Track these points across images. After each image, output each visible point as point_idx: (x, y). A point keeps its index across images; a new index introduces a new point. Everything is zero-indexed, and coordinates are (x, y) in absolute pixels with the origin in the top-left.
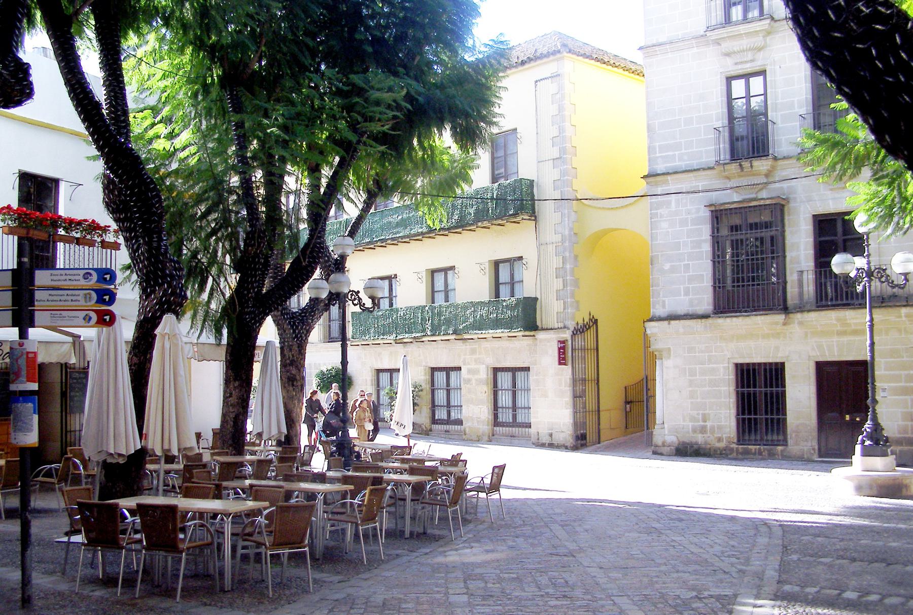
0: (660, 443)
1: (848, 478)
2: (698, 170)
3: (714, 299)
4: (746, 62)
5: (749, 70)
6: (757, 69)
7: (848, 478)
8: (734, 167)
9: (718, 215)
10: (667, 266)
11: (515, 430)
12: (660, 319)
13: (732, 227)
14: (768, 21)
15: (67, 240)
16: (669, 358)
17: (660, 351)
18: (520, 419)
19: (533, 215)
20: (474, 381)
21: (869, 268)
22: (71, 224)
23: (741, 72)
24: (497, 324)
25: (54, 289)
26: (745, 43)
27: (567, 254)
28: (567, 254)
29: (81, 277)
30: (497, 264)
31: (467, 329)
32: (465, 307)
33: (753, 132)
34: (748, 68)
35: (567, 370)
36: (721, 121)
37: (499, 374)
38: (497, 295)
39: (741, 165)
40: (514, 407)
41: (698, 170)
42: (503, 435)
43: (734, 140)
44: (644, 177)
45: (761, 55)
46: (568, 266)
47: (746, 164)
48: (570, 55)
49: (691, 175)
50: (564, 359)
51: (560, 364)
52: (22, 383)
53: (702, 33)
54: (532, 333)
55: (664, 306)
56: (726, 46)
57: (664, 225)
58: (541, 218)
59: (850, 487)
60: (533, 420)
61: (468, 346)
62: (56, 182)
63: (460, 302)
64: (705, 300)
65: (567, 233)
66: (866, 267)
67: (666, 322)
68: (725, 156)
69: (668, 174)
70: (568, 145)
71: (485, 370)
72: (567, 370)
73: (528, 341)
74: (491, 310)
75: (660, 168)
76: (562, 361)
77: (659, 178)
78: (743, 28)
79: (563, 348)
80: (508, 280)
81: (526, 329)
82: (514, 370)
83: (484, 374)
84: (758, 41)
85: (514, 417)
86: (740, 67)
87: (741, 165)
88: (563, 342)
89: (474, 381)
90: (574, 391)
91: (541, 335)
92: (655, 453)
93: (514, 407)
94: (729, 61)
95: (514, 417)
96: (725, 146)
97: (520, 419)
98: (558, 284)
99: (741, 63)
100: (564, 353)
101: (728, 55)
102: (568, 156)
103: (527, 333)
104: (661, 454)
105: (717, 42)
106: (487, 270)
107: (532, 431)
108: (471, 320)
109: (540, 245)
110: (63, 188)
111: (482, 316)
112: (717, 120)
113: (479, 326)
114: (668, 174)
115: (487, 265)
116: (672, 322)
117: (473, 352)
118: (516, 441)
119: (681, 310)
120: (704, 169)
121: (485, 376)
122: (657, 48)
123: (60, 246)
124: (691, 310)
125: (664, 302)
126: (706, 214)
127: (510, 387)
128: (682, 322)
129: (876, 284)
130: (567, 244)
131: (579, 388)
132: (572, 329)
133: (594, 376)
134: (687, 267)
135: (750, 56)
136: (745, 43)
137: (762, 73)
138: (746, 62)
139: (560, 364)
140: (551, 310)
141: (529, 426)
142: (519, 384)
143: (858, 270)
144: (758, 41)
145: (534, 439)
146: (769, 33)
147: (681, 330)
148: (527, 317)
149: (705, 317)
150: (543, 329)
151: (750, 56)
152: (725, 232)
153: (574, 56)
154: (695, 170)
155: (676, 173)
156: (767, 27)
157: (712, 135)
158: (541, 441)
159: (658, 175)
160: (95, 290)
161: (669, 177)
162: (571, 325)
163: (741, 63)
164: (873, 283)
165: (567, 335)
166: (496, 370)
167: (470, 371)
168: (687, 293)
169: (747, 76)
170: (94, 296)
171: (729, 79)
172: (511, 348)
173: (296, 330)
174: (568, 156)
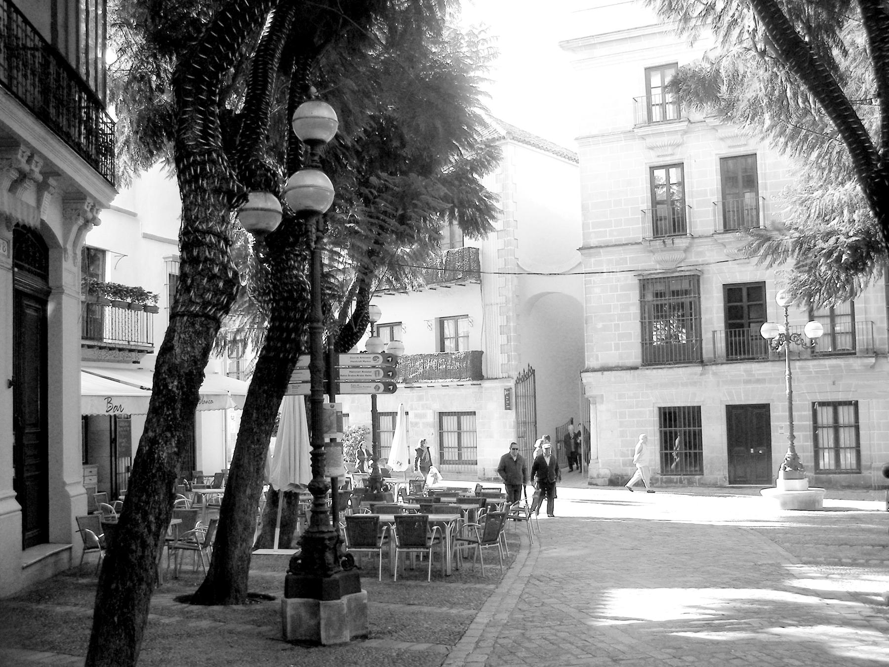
0: (595, 476)
1: (776, 497)
2: (627, 244)
3: (643, 352)
4: (667, 155)
5: (669, 162)
6: (676, 162)
7: (776, 497)
8: (658, 243)
9: (645, 283)
10: (600, 325)
11: (461, 467)
12: (594, 370)
13: (657, 294)
14: (686, 123)
15: (114, 304)
16: (602, 403)
17: (594, 397)
18: (465, 457)
19: (479, 281)
20: (421, 425)
21: (788, 333)
22: (118, 291)
23: (662, 163)
24: (446, 374)
25: (354, 367)
26: (666, 140)
27: (511, 314)
28: (511, 314)
29: (371, 359)
30: (441, 322)
31: (416, 379)
32: (414, 359)
33: (674, 214)
34: (669, 160)
35: (512, 414)
36: (646, 205)
37: (445, 418)
38: (442, 349)
39: (664, 242)
40: (459, 447)
41: (627, 244)
42: (449, 471)
43: (656, 220)
44: (579, 249)
45: (679, 149)
46: (512, 324)
47: (669, 241)
48: (512, 141)
49: (621, 248)
50: (509, 404)
51: (506, 409)
52: (333, 433)
53: (629, 129)
54: (479, 382)
55: (597, 359)
56: (650, 141)
57: (597, 290)
58: (485, 281)
59: (777, 503)
60: (479, 458)
61: (415, 393)
62: (104, 252)
63: (409, 354)
64: (634, 355)
65: (510, 295)
66: (785, 332)
67: (600, 373)
68: (649, 234)
69: (601, 247)
70: (511, 219)
71: (432, 415)
72: (512, 414)
73: (476, 388)
74: (440, 361)
75: (593, 242)
76: (508, 407)
77: (592, 251)
78: (664, 128)
79: (508, 395)
80: (453, 335)
81: (473, 379)
82: (459, 414)
83: (431, 418)
84: (677, 138)
85: (460, 455)
86: (661, 159)
87: (664, 242)
88: (509, 390)
89: (421, 425)
90: (518, 432)
91: (486, 384)
92: (590, 484)
93: (459, 447)
94: (652, 154)
95: (460, 455)
96: (649, 225)
97: (465, 457)
98: (503, 339)
99: (663, 156)
100: (509, 400)
101: (652, 148)
102: (511, 229)
103: (475, 382)
104: (597, 485)
105: (643, 138)
106: (434, 326)
107: (479, 467)
108: (421, 370)
109: (485, 306)
110: (109, 257)
111: (431, 367)
112: (643, 203)
113: (428, 375)
114: (601, 247)
115: (433, 322)
116: (605, 373)
117: (420, 398)
118: (463, 477)
119: (612, 362)
120: (632, 244)
121: (432, 420)
122: (590, 140)
123: (108, 310)
124: (621, 363)
125: (597, 355)
126: (636, 282)
127: (456, 428)
128: (614, 372)
129: (793, 345)
130: (511, 305)
131: (522, 429)
132: (515, 378)
133: (533, 420)
134: (617, 326)
135: (670, 151)
136: (666, 140)
137: (680, 165)
138: (667, 155)
139: (506, 409)
140: (497, 361)
141: (476, 463)
142: (464, 427)
143: (780, 335)
144: (677, 138)
145: (480, 474)
146: (686, 132)
147: (613, 379)
148: (475, 368)
149: (635, 368)
150: (488, 379)
151: (670, 151)
152: (649, 297)
153: (516, 142)
154: (624, 245)
155: (607, 246)
156: (685, 128)
157: (640, 216)
158: (487, 476)
159: (592, 248)
160: (383, 369)
161: (601, 250)
162: (515, 375)
163: (663, 156)
164: (791, 345)
165: (511, 384)
166: (441, 414)
167: (416, 416)
168: (617, 348)
169: (667, 167)
170: (382, 372)
171: (652, 169)
172: (457, 395)
173: (326, 381)
174: (511, 229)
